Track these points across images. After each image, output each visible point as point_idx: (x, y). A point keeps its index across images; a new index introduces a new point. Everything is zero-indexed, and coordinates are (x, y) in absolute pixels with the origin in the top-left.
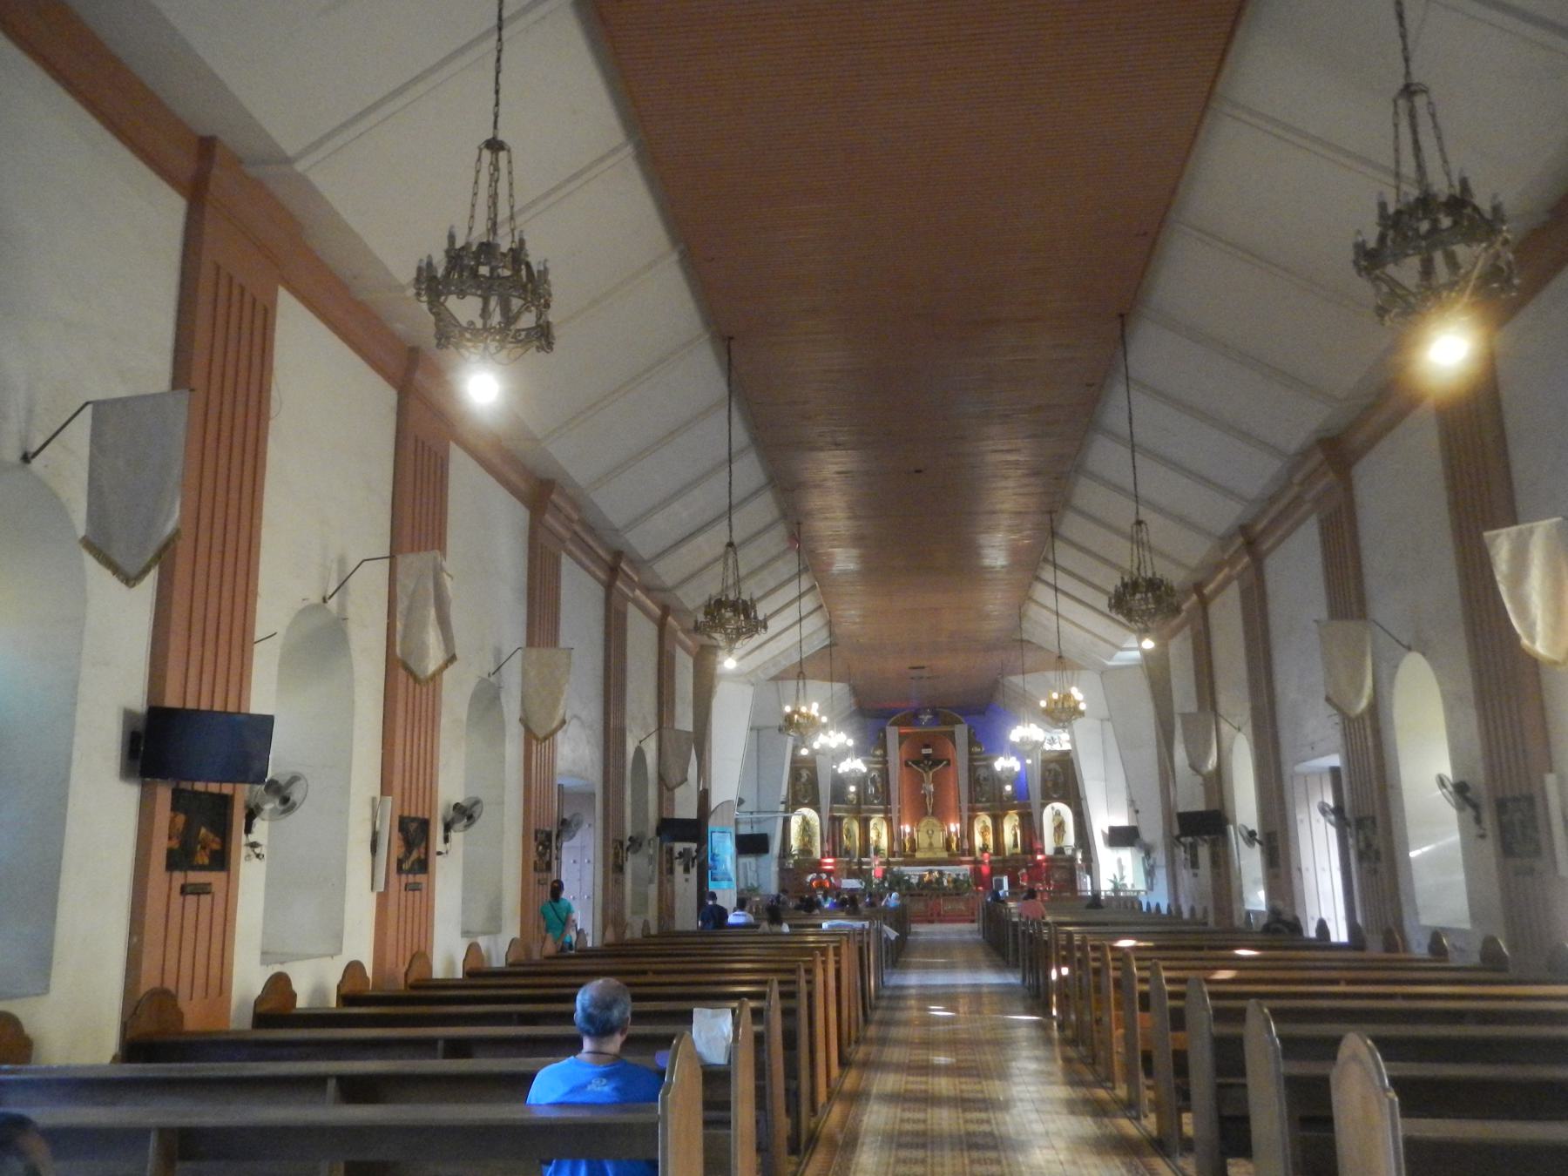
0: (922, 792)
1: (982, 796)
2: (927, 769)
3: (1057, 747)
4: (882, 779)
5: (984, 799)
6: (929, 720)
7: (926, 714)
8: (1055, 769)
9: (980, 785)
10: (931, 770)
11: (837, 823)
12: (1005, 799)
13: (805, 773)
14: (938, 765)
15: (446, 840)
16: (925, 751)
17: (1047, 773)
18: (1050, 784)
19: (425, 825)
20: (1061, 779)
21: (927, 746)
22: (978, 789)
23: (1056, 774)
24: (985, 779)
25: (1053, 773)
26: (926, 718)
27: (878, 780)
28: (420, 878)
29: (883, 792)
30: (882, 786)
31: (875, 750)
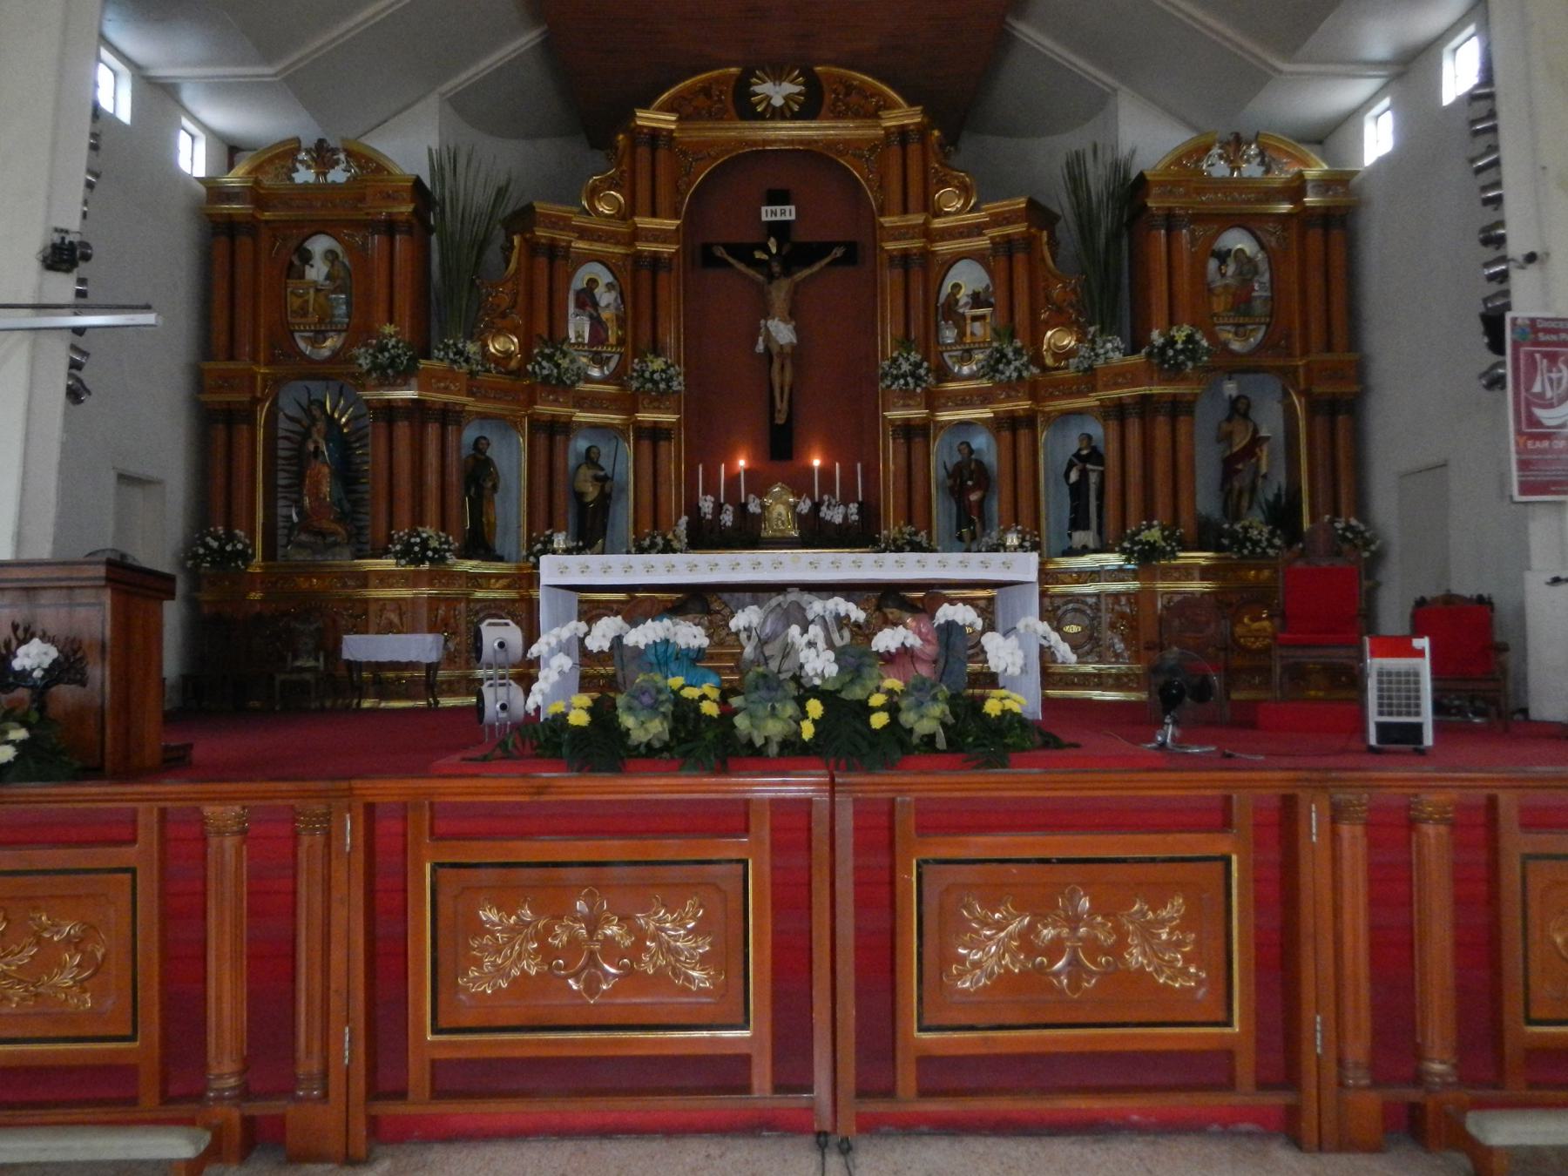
0: (760, 347)
1: (967, 356)
2: (776, 269)
3: (1252, 170)
4: (621, 294)
5: (966, 370)
6: (787, 98)
7: (778, 76)
8: (1241, 250)
9: (959, 322)
10: (787, 272)
11: (432, 431)
12: (1049, 361)
13: (319, 245)
14: (809, 264)
16: (769, 214)
17: (1213, 264)
18: (1219, 305)
20: (1260, 288)
22: (949, 335)
24: (977, 300)
25: (1231, 269)
27: (606, 298)
29: (621, 342)
30: (621, 322)
31: (594, 193)
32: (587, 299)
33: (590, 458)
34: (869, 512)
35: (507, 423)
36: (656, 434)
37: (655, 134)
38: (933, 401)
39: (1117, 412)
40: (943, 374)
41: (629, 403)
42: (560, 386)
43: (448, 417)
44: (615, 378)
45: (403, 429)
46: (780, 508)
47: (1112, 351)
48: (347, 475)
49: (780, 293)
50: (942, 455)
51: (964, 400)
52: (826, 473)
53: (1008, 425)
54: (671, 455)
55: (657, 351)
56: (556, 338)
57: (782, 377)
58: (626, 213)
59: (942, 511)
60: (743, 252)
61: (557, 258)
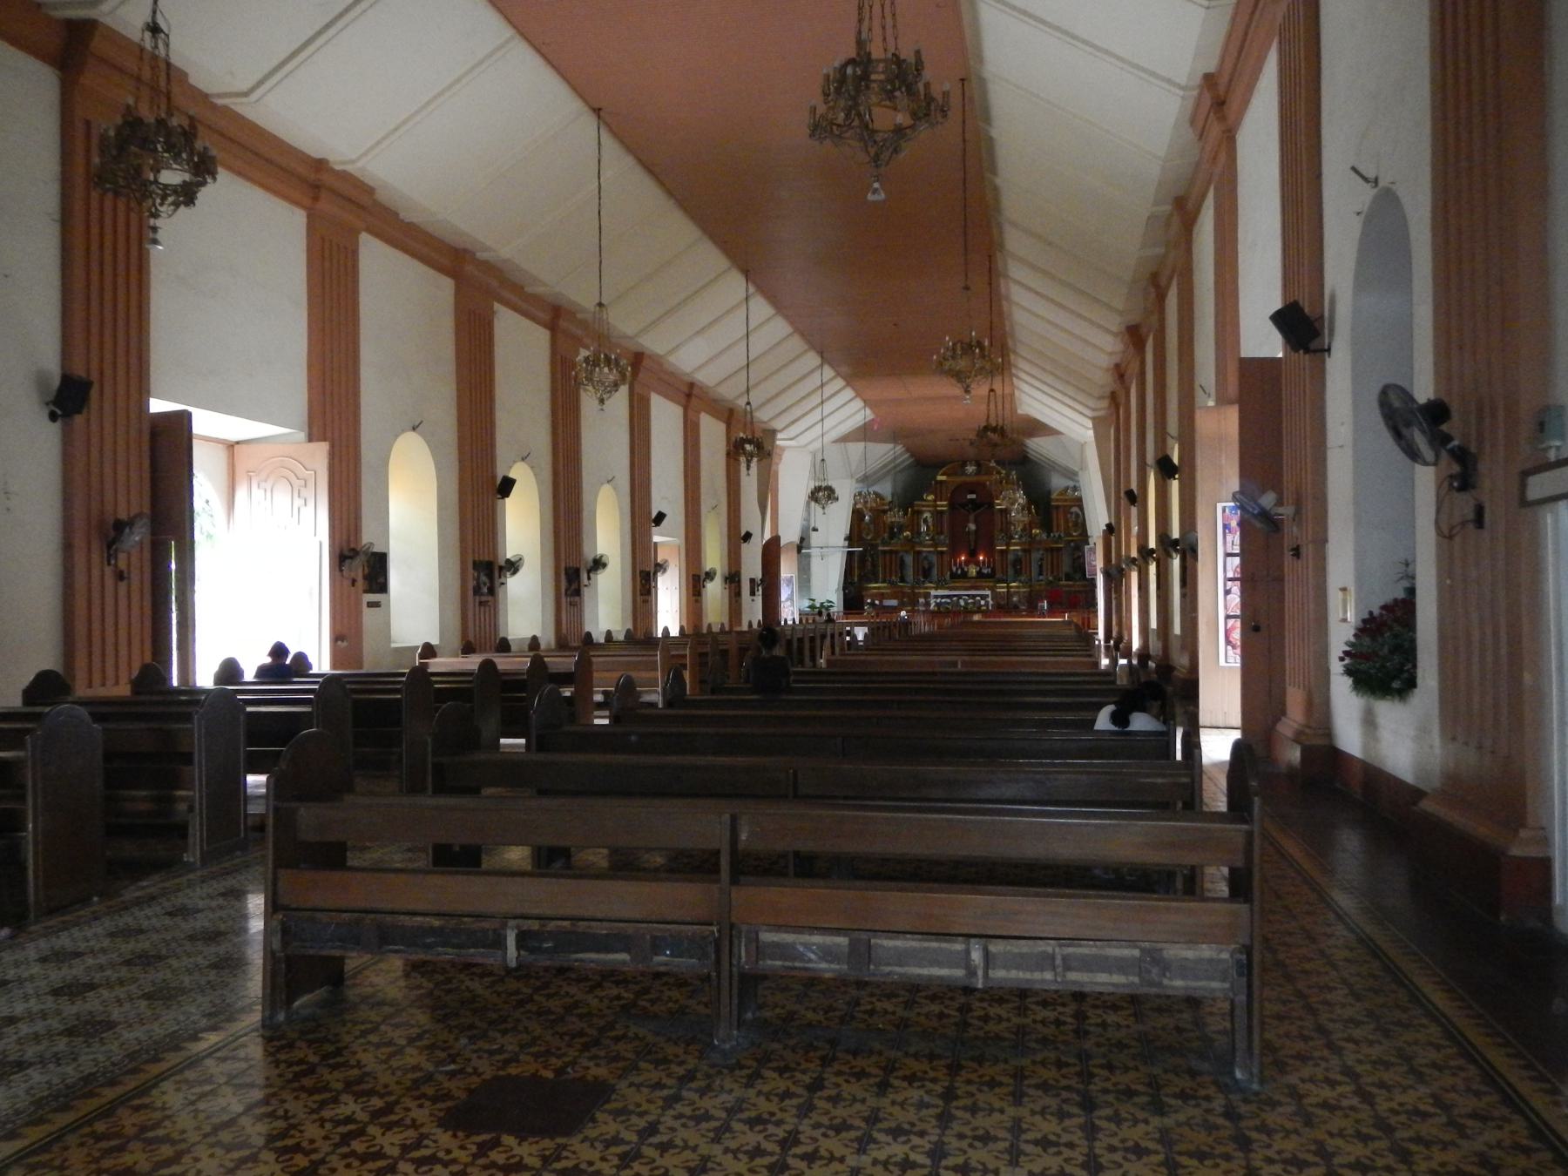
15: (589, 578)
16: (969, 497)
19: (577, 571)
21: (972, 492)
23: (1077, 515)
26: (971, 469)
27: (930, 520)
28: (577, 599)
32: (925, 521)
33: (926, 558)
34: (993, 570)
35: (907, 552)
36: (942, 552)
37: (941, 482)
38: (1008, 545)
39: (1046, 550)
40: (1012, 538)
41: (935, 545)
42: (921, 544)
43: (896, 552)
44: (932, 539)
45: (888, 557)
46: (973, 571)
47: (1044, 536)
48: (874, 565)
49: (972, 517)
50: (1011, 557)
51: (1015, 544)
52: (984, 561)
53: (1024, 551)
54: (946, 558)
55: (942, 533)
56: (919, 533)
57: (972, 538)
58: (935, 501)
59: (1011, 571)
60: (963, 506)
61: (920, 513)
